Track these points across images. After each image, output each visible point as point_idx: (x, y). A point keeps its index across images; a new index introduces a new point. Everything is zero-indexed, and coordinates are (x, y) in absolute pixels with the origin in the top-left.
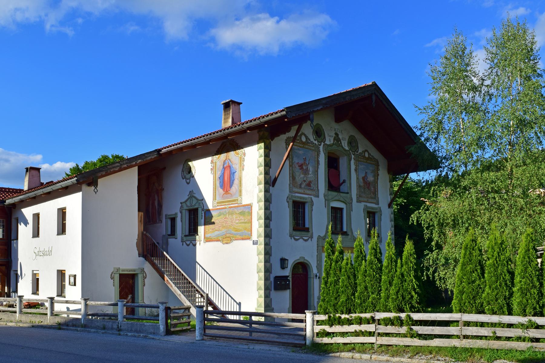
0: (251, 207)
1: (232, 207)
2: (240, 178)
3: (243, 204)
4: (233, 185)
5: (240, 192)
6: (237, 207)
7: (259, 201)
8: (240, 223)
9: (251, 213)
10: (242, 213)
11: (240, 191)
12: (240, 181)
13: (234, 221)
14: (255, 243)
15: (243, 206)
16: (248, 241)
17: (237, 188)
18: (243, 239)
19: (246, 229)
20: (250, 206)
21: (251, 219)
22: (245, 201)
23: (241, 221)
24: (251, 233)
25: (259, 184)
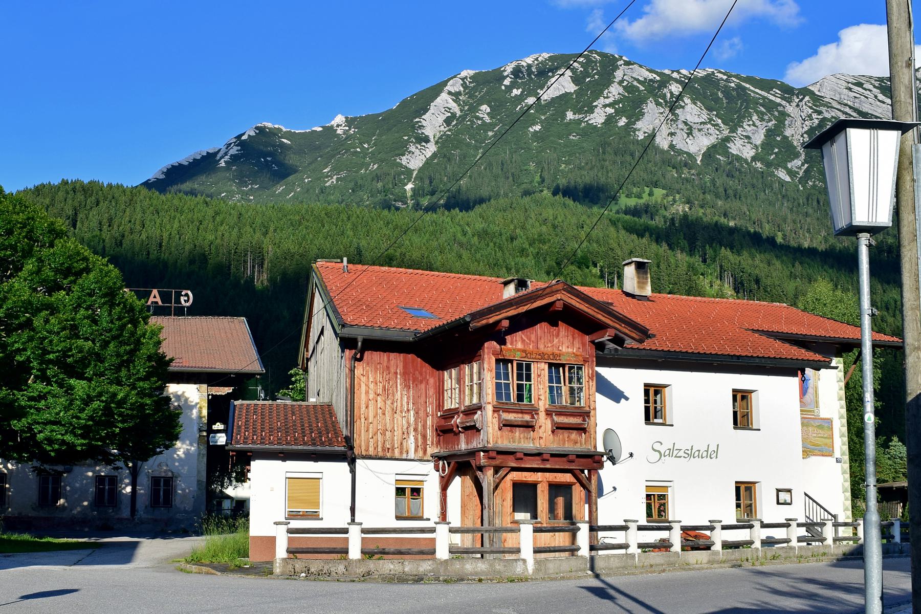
0: (832, 422)
1: (806, 418)
2: (816, 387)
3: (822, 416)
4: (807, 394)
5: (817, 403)
6: (814, 418)
7: (841, 417)
8: (819, 437)
9: (832, 428)
10: (820, 427)
11: (817, 402)
12: (816, 391)
13: (810, 434)
14: (838, 461)
15: (821, 419)
16: (829, 458)
17: (812, 398)
18: (823, 455)
19: (826, 444)
20: (829, 421)
21: (833, 435)
22: (824, 413)
23: (820, 435)
24: (833, 450)
25: (840, 399)
